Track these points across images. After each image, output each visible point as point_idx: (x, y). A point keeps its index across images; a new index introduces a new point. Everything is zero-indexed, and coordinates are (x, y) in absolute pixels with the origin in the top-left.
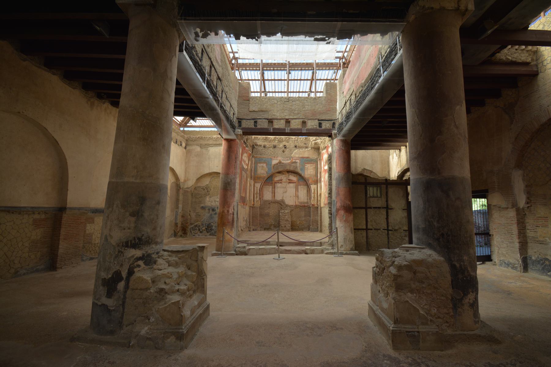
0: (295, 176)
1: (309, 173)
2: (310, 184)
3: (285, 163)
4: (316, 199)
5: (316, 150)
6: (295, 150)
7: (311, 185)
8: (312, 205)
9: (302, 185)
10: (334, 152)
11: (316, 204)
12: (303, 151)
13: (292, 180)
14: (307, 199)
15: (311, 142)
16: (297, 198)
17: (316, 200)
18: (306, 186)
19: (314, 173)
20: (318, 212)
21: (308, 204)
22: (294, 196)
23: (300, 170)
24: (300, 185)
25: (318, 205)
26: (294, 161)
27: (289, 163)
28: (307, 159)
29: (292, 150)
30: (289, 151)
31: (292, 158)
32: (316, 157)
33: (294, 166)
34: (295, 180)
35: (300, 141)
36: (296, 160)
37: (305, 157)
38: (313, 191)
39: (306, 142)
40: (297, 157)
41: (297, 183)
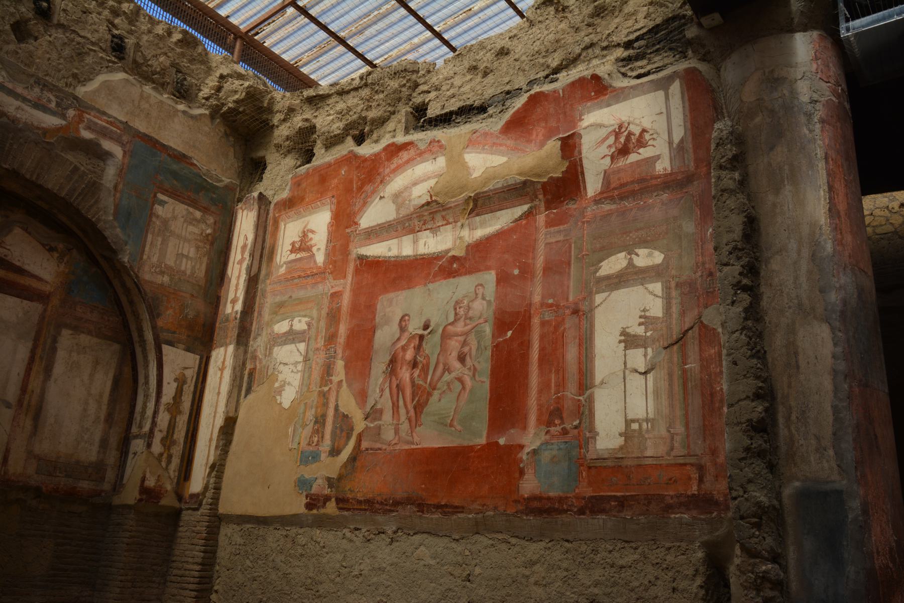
0: (51, 250)
1: (170, 261)
2: (164, 336)
3: (15, 120)
4: (177, 451)
5: (231, 139)
6: (111, 70)
7: (171, 344)
8: (144, 490)
9: (89, 333)
10: (809, 116)
11: (169, 487)
12: (161, 102)
13: (20, 271)
14: (104, 443)
15: (222, 77)
16: (28, 423)
17: (176, 462)
18: (116, 347)
19: (201, 271)
20: (170, 538)
21: (103, 479)
22: (8, 405)
23: (116, 214)
24: (76, 329)
25: (180, 498)
26: (86, 135)
27: (46, 132)
28: (175, 167)
29: (89, 60)
30: (67, 52)
31: (82, 106)
32: (227, 181)
33: (76, 169)
34: (47, 276)
35: (150, 32)
36: (104, 133)
37: (165, 148)
38: (169, 391)
39: (184, 63)
40: (114, 122)
41: (55, 301)
